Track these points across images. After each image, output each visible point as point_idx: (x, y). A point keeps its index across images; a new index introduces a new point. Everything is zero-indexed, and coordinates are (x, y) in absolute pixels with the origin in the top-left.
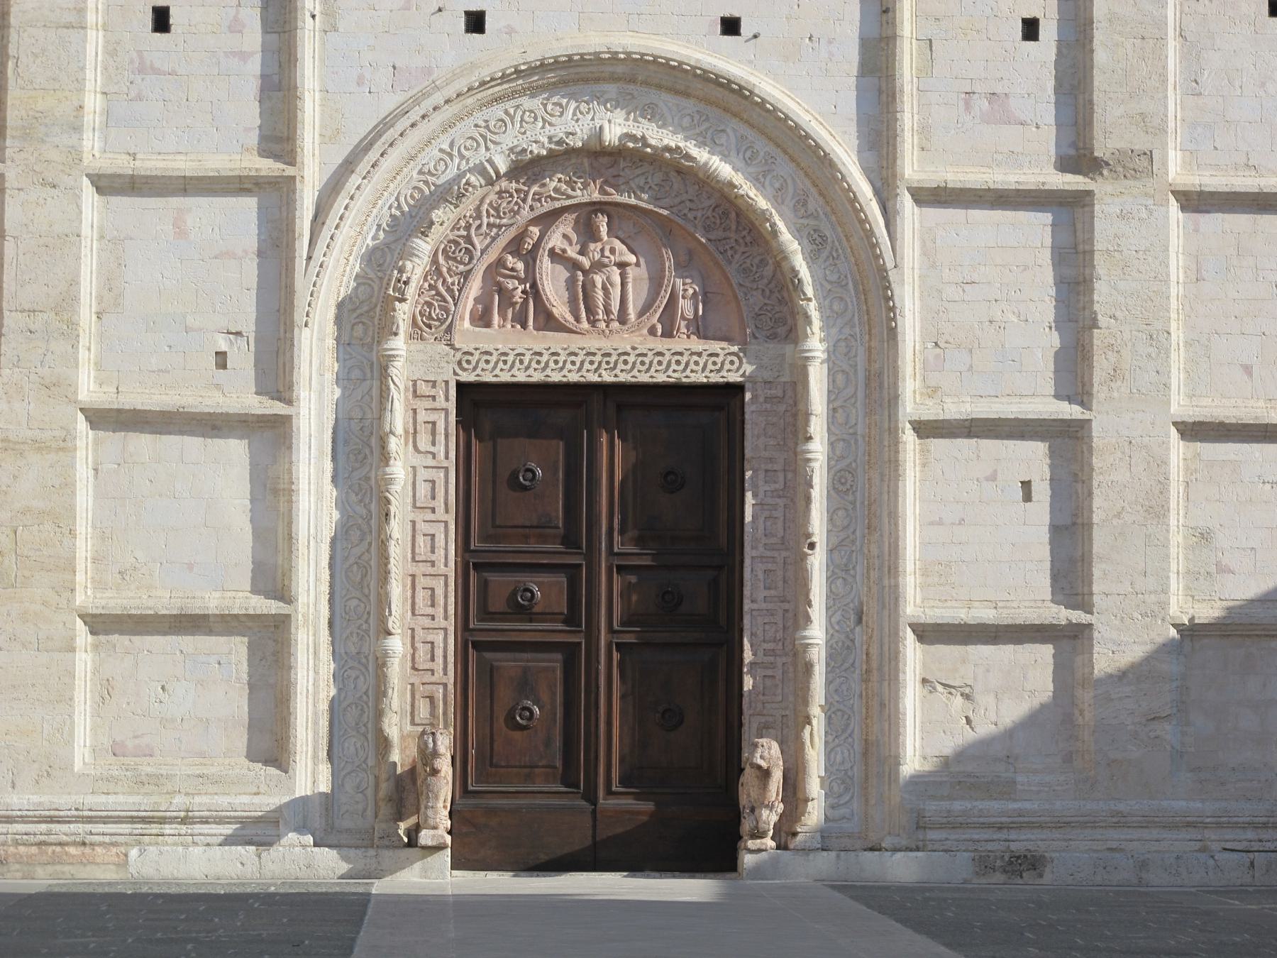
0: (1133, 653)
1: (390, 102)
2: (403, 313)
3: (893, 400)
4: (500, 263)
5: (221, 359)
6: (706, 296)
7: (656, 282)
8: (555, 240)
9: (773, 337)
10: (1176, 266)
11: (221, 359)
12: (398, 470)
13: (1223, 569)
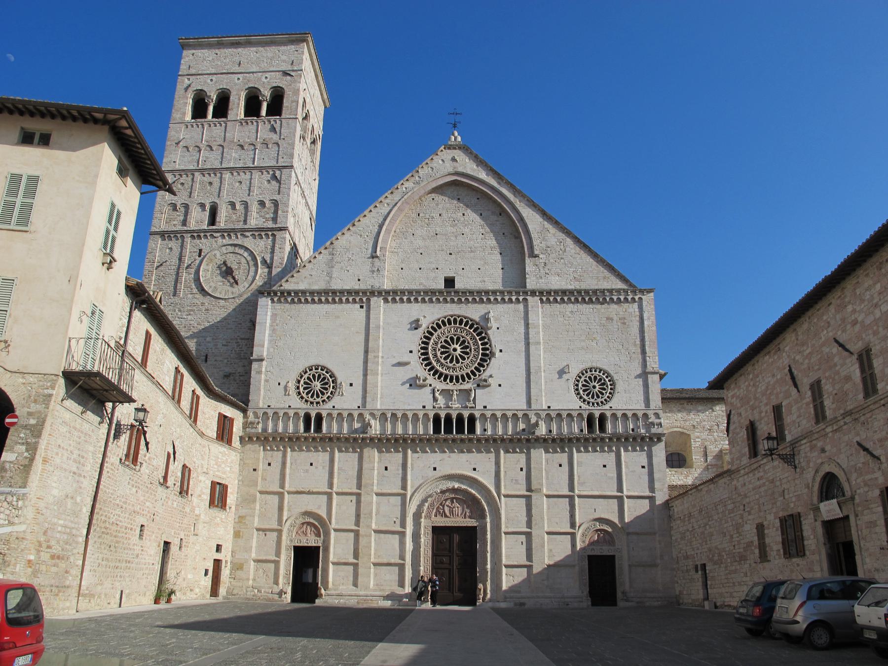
0: (540, 569)
1: (421, 482)
2: (423, 515)
3: (501, 529)
4: (439, 507)
5: (395, 522)
6: (471, 512)
7: (463, 511)
8: (447, 503)
9: (481, 518)
10: (545, 506)
11: (395, 522)
12: (422, 540)
13: (554, 556)
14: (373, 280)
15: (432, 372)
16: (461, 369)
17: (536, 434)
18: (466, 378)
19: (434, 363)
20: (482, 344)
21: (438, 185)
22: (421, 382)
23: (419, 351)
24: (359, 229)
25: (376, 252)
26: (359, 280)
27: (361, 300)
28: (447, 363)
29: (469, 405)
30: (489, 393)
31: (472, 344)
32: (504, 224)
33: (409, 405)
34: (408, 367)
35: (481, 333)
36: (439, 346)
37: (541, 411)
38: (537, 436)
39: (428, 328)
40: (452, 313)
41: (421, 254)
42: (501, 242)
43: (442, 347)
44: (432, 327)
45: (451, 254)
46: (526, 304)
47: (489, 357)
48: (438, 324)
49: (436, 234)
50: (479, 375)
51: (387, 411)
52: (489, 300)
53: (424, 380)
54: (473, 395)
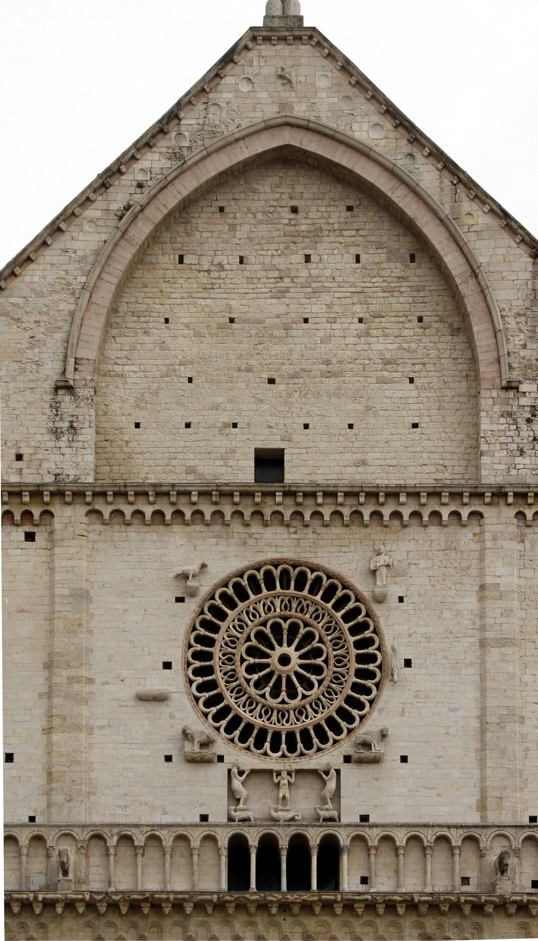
14: (59, 458)
15: (224, 723)
16: (300, 713)
17: (499, 892)
18: (316, 740)
19: (230, 699)
20: (358, 645)
21: (234, 161)
22: (197, 748)
23: (189, 664)
24: (13, 300)
25: (64, 372)
26: (19, 457)
27: (27, 515)
28: (263, 696)
29: (323, 814)
30: (376, 779)
31: (329, 644)
32: (423, 288)
33: (165, 813)
34: (163, 709)
35: (356, 611)
36: (243, 648)
37: (513, 830)
38: (501, 897)
39: (213, 598)
40: (277, 556)
41: (190, 380)
42: (413, 346)
43: (251, 651)
44: (224, 597)
45: (271, 381)
46: (477, 530)
47: (377, 680)
48: (237, 587)
49: (232, 320)
50: (350, 731)
51: (106, 830)
52: (377, 515)
53: (206, 744)
54: (332, 785)
